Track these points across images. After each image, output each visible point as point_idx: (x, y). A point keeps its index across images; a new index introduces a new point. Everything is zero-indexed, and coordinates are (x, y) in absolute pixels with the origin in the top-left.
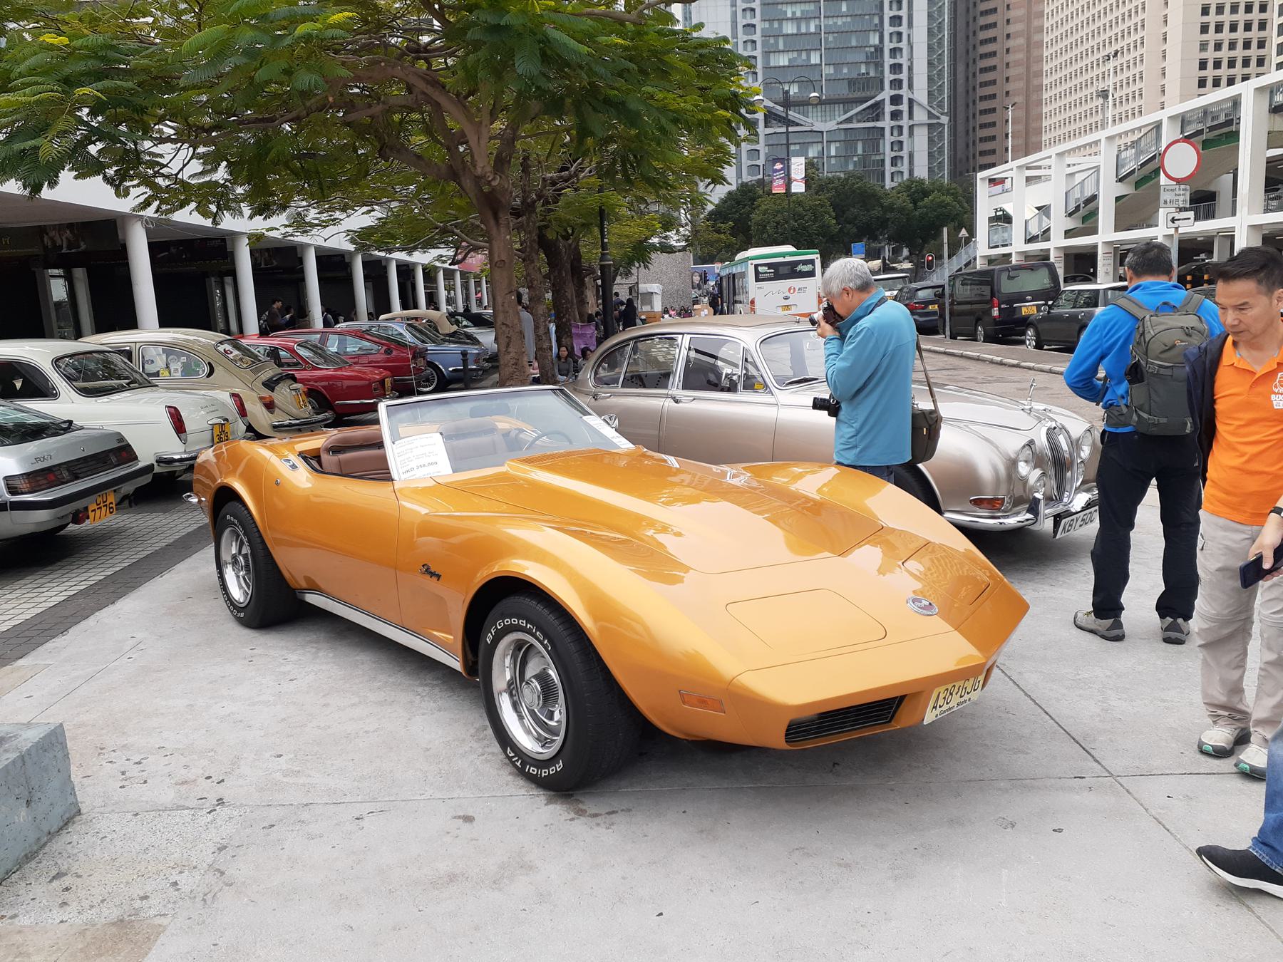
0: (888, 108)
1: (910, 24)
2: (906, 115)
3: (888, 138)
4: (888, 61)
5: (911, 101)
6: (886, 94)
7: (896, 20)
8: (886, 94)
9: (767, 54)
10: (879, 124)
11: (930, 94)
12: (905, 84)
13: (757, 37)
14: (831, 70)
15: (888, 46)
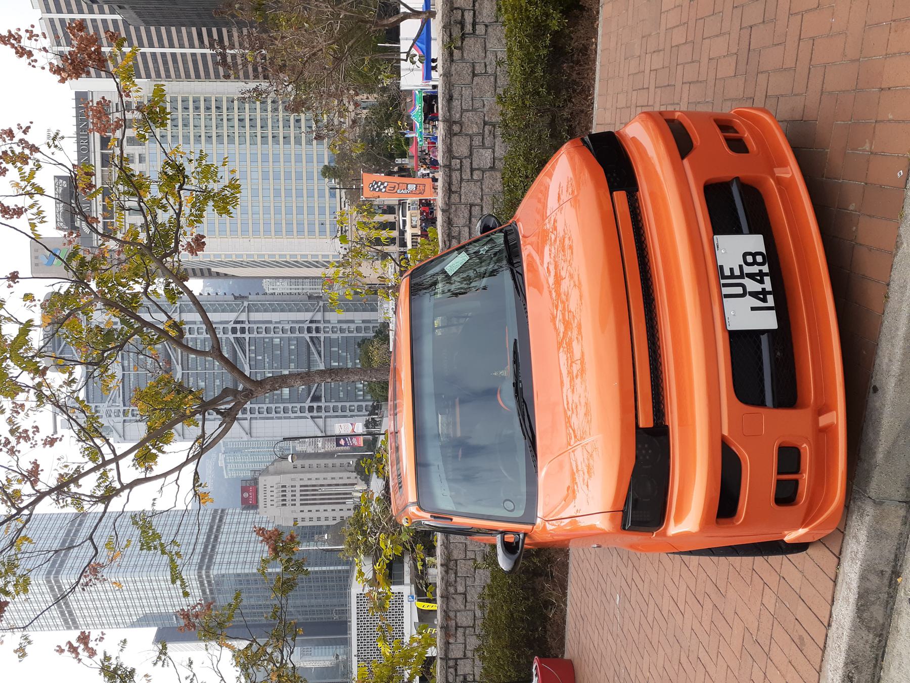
0: (314, 334)
1: (270, 322)
2: (318, 325)
3: (331, 335)
4: (289, 334)
5: (311, 322)
6: (307, 336)
7: (267, 330)
8: (307, 336)
9: (283, 401)
10: (322, 340)
11: (307, 310)
12: (301, 325)
13: (273, 406)
14: (292, 365)
15: (281, 334)
